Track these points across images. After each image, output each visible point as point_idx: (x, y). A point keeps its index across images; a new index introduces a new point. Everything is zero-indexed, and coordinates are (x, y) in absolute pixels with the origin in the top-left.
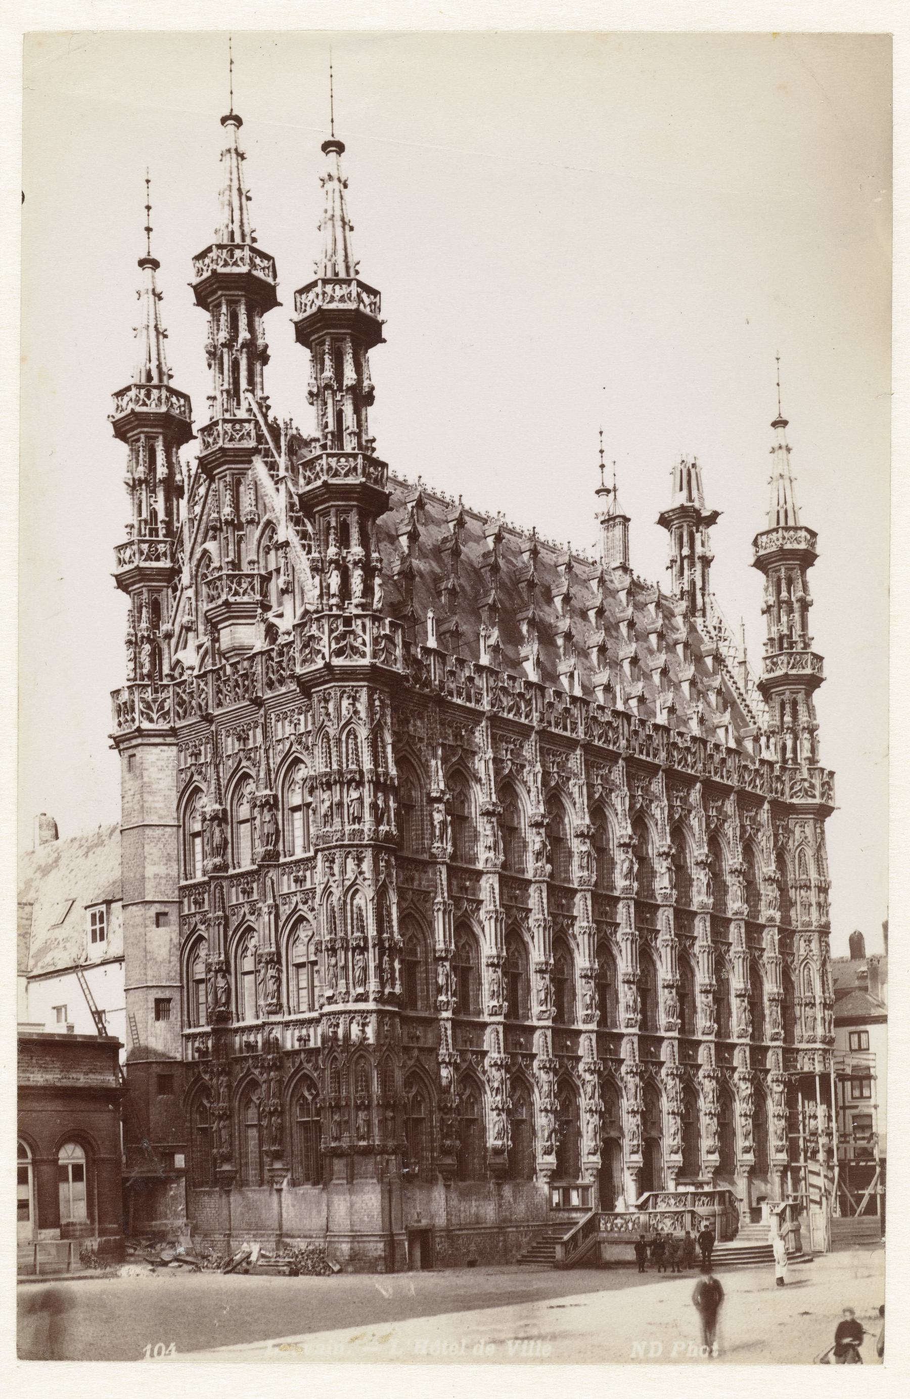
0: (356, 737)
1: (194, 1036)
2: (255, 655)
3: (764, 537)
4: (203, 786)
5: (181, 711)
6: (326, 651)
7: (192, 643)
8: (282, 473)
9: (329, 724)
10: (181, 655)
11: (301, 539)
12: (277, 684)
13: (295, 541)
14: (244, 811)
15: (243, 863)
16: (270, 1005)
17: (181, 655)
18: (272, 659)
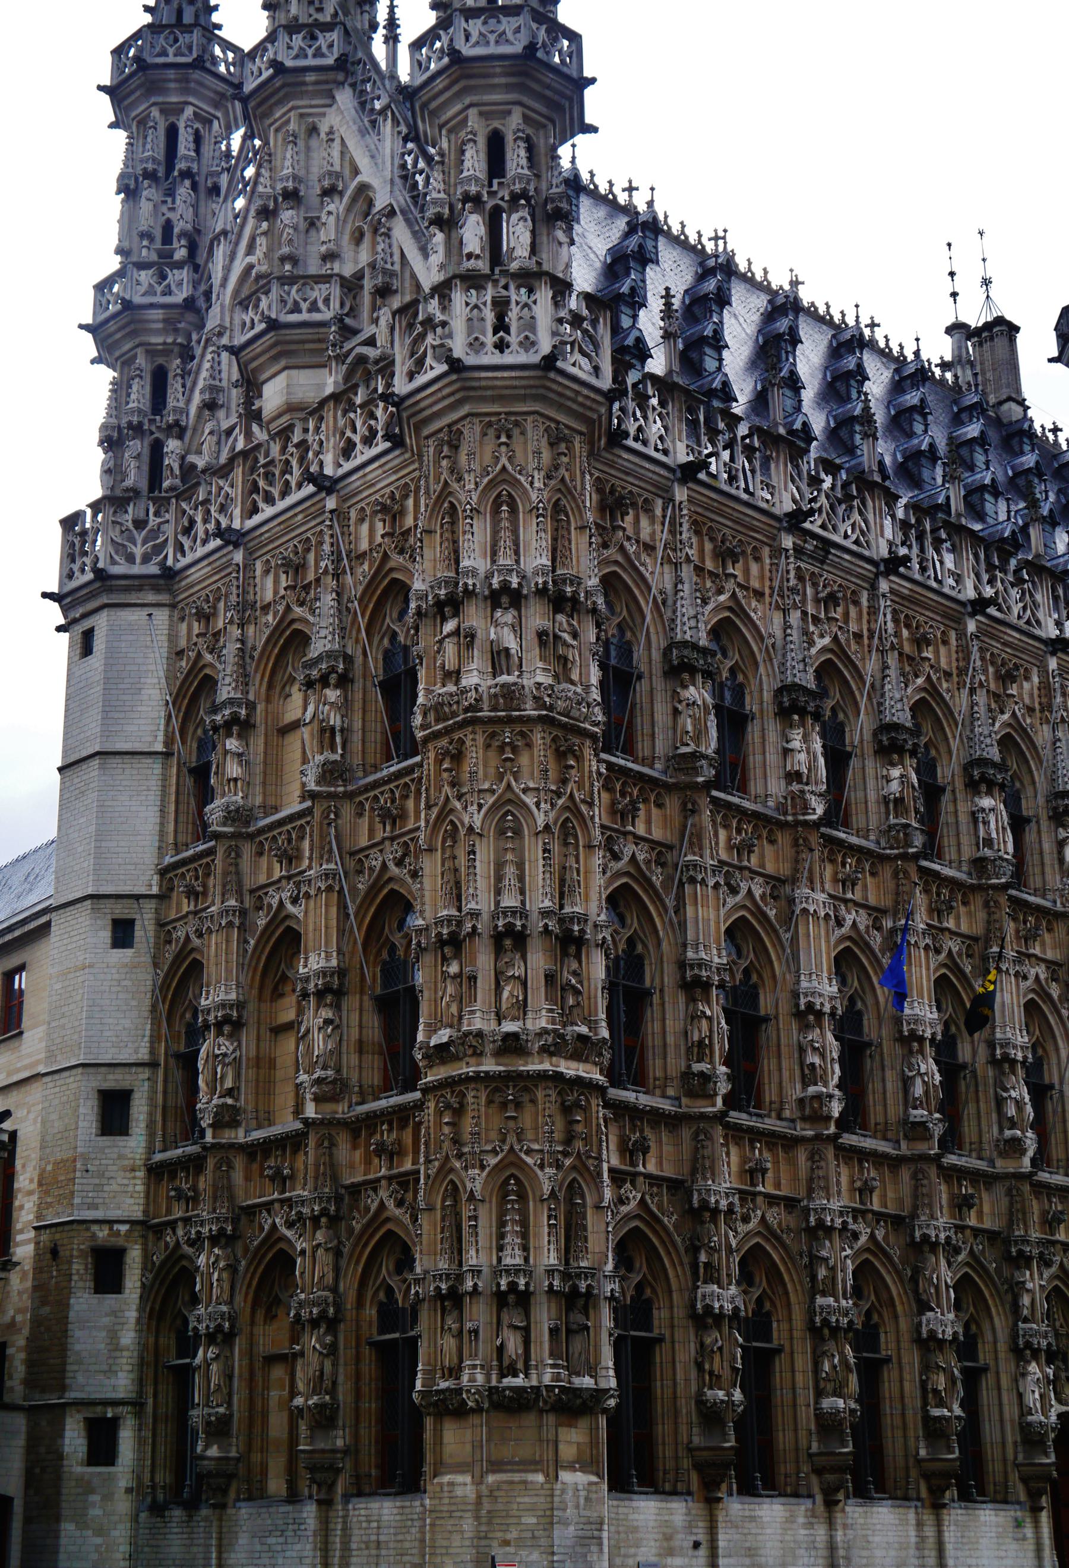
0: (513, 510)
2: (323, 403)
16: (319, 1081)
18: (351, 407)
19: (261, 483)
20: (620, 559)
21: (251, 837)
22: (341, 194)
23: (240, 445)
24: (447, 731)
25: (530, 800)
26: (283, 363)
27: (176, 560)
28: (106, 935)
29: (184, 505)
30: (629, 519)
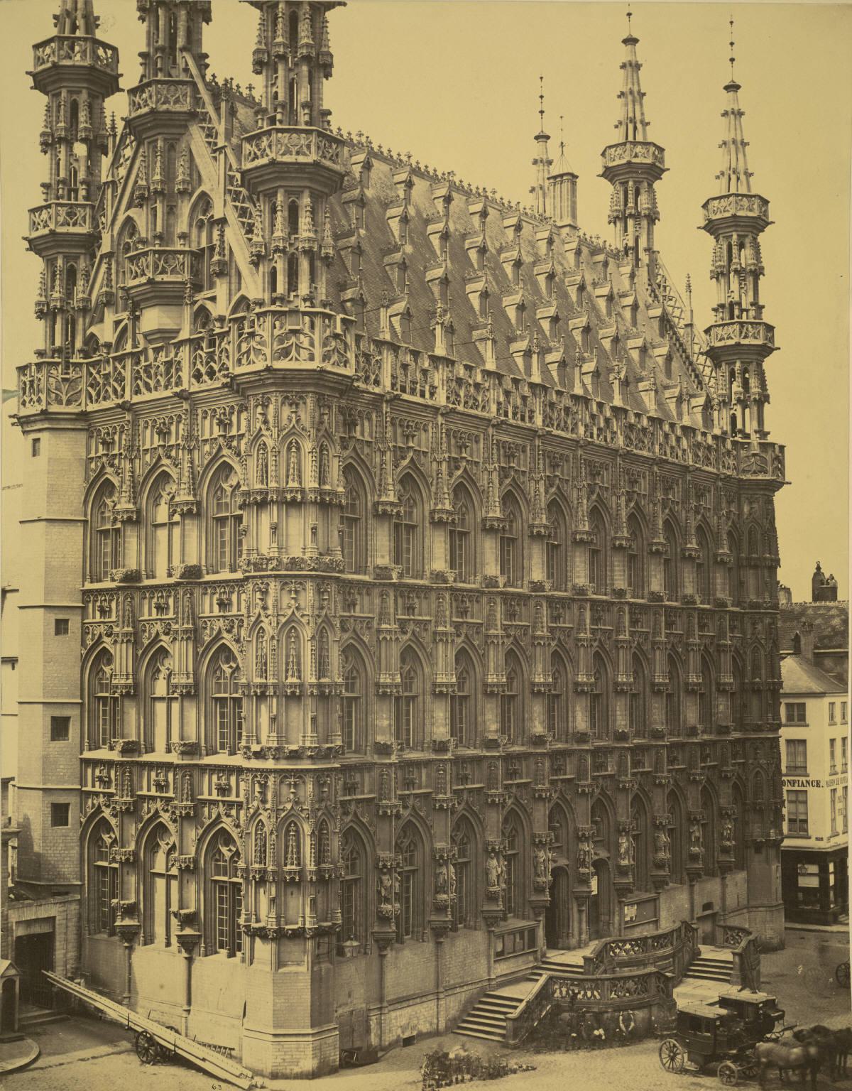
0: (298, 449)
1: (95, 763)
2: (182, 343)
3: (716, 202)
4: (115, 480)
5: (94, 394)
6: (267, 351)
7: (110, 317)
8: (221, 142)
9: (267, 433)
10: (93, 329)
11: (240, 216)
12: (205, 377)
13: (232, 217)
14: (162, 514)
15: (158, 573)
17: (93, 329)
19: (144, 376)
20: (353, 455)
21: (139, 588)
22: (191, 195)
23: (129, 348)
24: (261, 577)
25: (304, 620)
26: (155, 301)
27: (87, 405)
28: (53, 630)
29: (91, 369)
30: (358, 428)
